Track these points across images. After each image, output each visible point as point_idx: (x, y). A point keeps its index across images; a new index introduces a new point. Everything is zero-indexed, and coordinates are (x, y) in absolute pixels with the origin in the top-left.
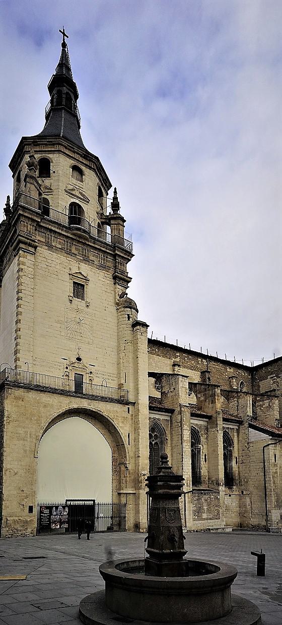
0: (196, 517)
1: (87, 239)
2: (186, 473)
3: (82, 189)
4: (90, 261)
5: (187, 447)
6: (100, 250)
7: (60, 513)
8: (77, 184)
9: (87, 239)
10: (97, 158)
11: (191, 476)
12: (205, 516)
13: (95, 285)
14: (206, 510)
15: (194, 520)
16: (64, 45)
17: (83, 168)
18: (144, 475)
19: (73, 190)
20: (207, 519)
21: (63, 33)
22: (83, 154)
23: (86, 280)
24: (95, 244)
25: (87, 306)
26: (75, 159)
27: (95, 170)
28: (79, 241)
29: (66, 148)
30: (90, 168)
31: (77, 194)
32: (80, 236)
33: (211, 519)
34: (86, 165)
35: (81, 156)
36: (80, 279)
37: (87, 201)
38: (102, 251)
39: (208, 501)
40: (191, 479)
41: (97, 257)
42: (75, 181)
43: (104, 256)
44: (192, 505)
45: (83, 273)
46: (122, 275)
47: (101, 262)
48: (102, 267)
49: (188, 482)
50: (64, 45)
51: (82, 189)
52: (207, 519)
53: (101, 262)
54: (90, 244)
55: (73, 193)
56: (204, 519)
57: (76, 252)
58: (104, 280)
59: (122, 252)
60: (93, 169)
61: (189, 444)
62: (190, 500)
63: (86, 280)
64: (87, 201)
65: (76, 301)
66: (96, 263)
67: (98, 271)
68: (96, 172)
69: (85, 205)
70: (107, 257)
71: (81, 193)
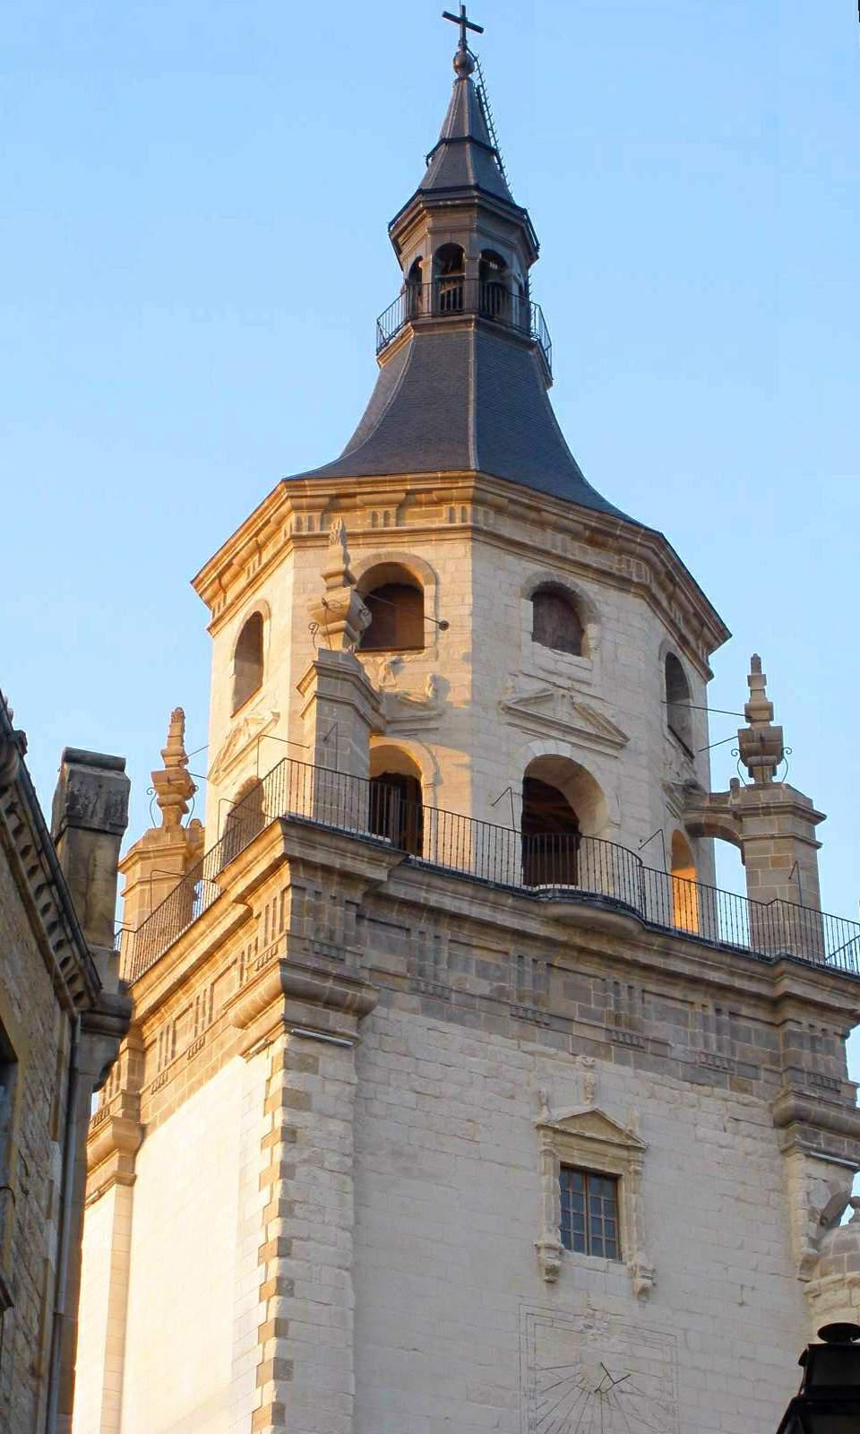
1: (623, 937)
3: (585, 689)
4: (650, 1047)
6: (694, 981)
8: (562, 667)
9: (623, 937)
10: (658, 539)
13: (680, 1168)
16: (465, 65)
17: (587, 588)
21: (463, 21)
22: (586, 527)
23: (628, 1148)
24: (667, 955)
25: (644, 1291)
26: (547, 553)
27: (647, 588)
28: (582, 951)
29: (500, 510)
30: (623, 583)
31: (562, 713)
32: (589, 928)
34: (603, 575)
35: (576, 536)
36: (596, 1146)
37: (616, 741)
38: (709, 984)
41: (682, 1020)
42: (546, 656)
43: (718, 1011)
45: (611, 1116)
46: (828, 1103)
47: (706, 1044)
48: (707, 1071)
50: (465, 65)
51: (585, 689)
53: (706, 1044)
54: (643, 958)
55: (544, 711)
57: (573, 1008)
58: (726, 1138)
59: (814, 983)
60: (639, 585)
63: (628, 1148)
64: (616, 741)
65: (582, 1263)
66: (678, 1050)
67: (691, 1094)
68: (653, 597)
69: (599, 759)
70: (733, 1014)
71: (584, 712)
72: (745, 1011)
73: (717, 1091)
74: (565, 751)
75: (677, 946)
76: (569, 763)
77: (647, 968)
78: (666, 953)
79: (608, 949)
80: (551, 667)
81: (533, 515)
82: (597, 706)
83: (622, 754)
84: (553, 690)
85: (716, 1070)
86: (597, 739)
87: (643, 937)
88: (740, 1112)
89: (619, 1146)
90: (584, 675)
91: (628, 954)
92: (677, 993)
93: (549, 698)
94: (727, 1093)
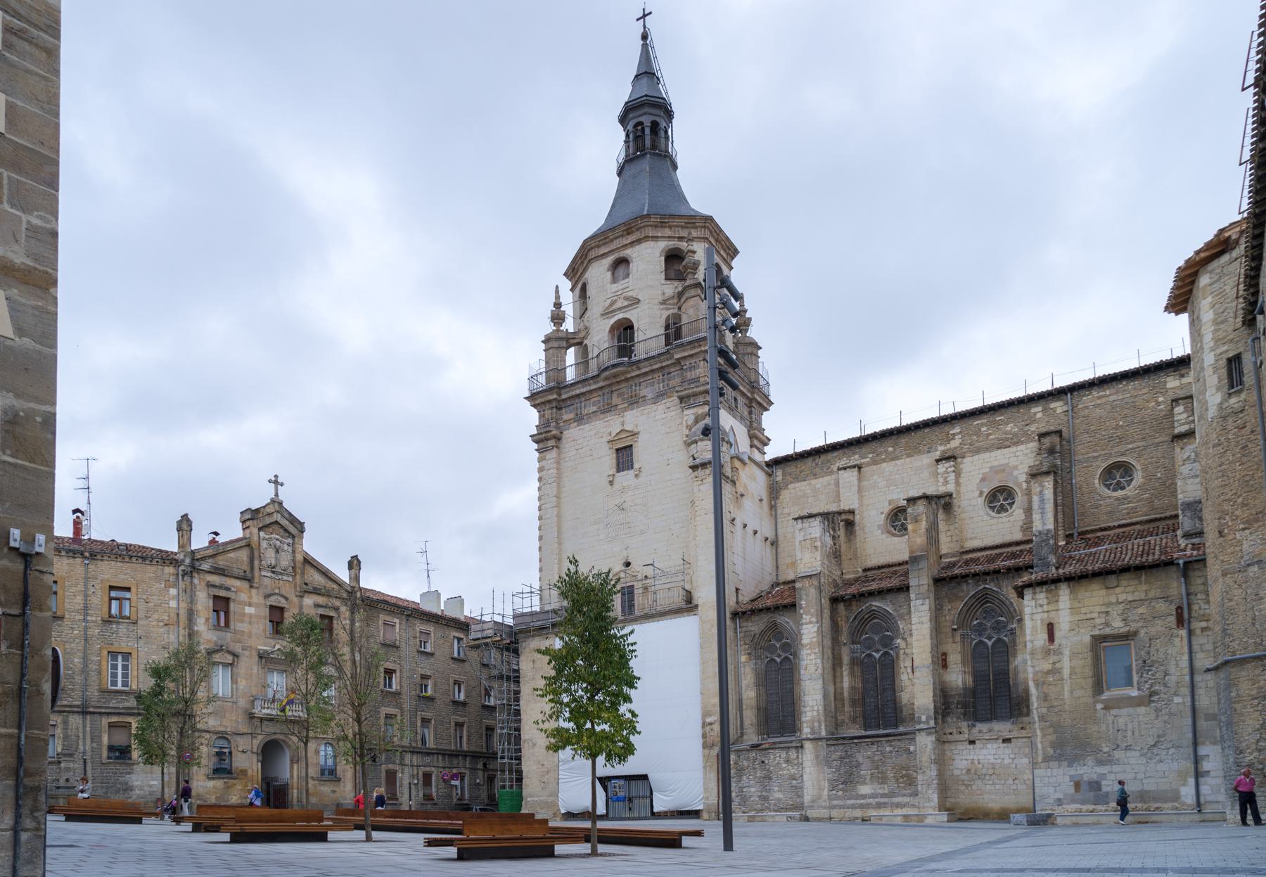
2: (808, 709)
3: (627, 290)
5: (813, 656)
6: (653, 371)
8: (620, 287)
18: (710, 724)
19: (612, 304)
38: (657, 369)
43: (663, 375)
48: (660, 396)
49: (816, 724)
54: (633, 374)
55: (615, 307)
58: (664, 416)
61: (817, 650)
66: (650, 396)
71: (626, 299)
72: (672, 370)
73: (663, 402)
74: (620, 316)
75: (640, 365)
78: (639, 369)
80: (616, 289)
81: (607, 240)
82: (630, 294)
83: (640, 305)
84: (615, 298)
85: (662, 395)
86: (630, 305)
88: (668, 405)
90: (627, 285)
91: (629, 376)
92: (650, 377)
93: (616, 301)
94: (666, 401)
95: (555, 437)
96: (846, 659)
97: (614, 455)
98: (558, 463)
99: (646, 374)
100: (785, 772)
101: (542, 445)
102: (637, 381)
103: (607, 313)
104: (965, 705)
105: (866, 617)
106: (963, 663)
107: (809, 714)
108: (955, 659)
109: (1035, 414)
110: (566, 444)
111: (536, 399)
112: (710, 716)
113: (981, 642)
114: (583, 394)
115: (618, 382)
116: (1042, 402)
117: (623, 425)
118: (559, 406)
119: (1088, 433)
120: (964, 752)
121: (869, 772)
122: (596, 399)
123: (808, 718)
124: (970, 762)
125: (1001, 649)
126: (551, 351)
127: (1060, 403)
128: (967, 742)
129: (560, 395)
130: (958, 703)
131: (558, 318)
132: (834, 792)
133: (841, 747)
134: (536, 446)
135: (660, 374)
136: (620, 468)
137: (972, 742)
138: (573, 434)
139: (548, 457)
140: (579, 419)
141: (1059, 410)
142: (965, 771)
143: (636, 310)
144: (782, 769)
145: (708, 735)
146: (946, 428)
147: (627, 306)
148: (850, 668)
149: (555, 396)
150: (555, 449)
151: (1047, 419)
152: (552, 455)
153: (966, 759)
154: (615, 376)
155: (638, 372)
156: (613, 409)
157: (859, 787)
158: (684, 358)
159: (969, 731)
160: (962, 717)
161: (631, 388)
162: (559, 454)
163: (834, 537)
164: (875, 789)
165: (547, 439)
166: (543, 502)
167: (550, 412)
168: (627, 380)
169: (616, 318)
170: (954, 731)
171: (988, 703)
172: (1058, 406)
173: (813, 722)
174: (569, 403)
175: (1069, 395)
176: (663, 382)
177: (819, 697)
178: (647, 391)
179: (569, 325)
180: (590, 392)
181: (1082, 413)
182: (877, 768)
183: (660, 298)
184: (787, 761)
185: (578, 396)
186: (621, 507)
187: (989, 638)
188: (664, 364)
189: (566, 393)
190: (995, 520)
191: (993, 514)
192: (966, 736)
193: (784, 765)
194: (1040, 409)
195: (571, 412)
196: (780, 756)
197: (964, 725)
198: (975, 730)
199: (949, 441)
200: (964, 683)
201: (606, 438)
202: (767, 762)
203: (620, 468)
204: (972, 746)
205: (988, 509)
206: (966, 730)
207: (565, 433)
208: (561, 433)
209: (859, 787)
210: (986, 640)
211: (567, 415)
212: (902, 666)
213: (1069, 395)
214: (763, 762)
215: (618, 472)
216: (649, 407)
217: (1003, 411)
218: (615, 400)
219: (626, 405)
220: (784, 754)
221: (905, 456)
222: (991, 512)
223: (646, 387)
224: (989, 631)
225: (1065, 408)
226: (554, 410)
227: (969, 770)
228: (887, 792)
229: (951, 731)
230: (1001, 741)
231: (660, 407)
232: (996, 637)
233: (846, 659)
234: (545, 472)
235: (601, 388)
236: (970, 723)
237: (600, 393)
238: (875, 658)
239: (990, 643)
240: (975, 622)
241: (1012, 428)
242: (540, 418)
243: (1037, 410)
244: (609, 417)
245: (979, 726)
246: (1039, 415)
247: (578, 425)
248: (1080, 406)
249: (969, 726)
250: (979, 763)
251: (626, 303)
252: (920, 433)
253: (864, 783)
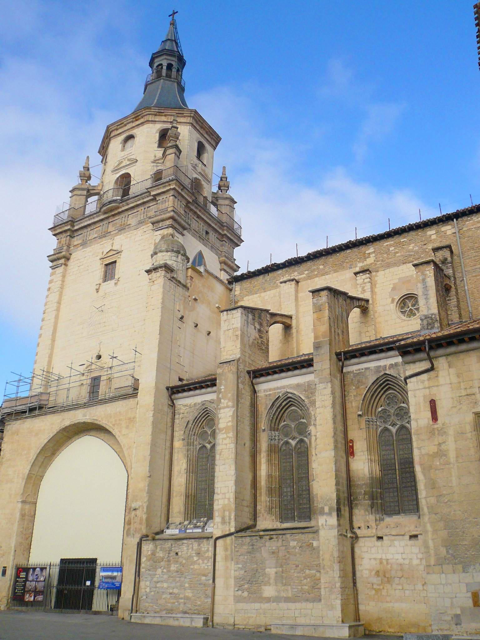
0: (246, 594)
1: (118, 208)
2: (220, 496)
7: (37, 578)
11: (232, 500)
12: (269, 591)
14: (273, 576)
15: (238, 600)
20: (277, 600)
33: (287, 600)
39: (281, 554)
40: (233, 506)
44: (233, 566)
49: (227, 513)
52: (277, 600)
54: (123, 209)
56: (268, 600)
62: (229, 553)
75: (128, 202)
76: (125, 173)
77: (127, 210)
78: (128, 204)
79: (116, 212)
87: (121, 204)
89: (116, 254)
91: (120, 210)
95: (64, 257)
96: (264, 445)
97: (103, 269)
98: (64, 276)
99: (133, 208)
100: (196, 567)
101: (55, 263)
102: (126, 214)
103: (115, 170)
104: (372, 498)
105: (283, 404)
106: (369, 449)
107: (221, 502)
108: (360, 446)
109: (430, 236)
110: (70, 263)
111: (56, 230)
112: (136, 501)
113: (386, 429)
114: (89, 225)
115: (113, 215)
116: (435, 227)
117: (112, 246)
118: (72, 233)
119: (473, 249)
120: (373, 550)
121: (275, 570)
122: (98, 229)
123: (220, 507)
124: (378, 561)
125: (405, 437)
126: (74, 197)
127: (449, 227)
128: (375, 538)
129: (73, 226)
130: (365, 494)
131: (86, 176)
132: (240, 592)
133: (248, 539)
134: (51, 264)
135: (143, 208)
136: (105, 279)
137: (380, 538)
138: (78, 255)
139: (57, 272)
140: (84, 244)
141: (449, 232)
142: (374, 573)
143: (134, 167)
144: (194, 563)
145: (132, 521)
146: (363, 248)
147: (129, 165)
148: (268, 455)
149: (69, 227)
150: (63, 266)
151: (440, 240)
152: (60, 270)
153: (375, 559)
154: (111, 210)
155: (126, 207)
156: (107, 235)
157: (263, 587)
158: (159, 194)
159: (377, 526)
160: (369, 509)
161: (122, 219)
162: (65, 270)
163: (260, 331)
164: (279, 592)
165: (59, 259)
166: (47, 307)
167: (65, 239)
168: (119, 213)
169: (121, 173)
170: (362, 525)
171: (396, 494)
172: (448, 229)
173: (224, 511)
174: (80, 232)
175: (455, 220)
176: (144, 213)
177: (231, 484)
178: (132, 220)
179: (93, 182)
180: (94, 223)
181: (467, 235)
182: (281, 566)
183: (153, 158)
184: (198, 554)
185: (85, 227)
186: (100, 309)
187: (394, 425)
188: (145, 200)
189: (77, 225)
190: (406, 322)
191: (405, 318)
192: (374, 531)
193: (195, 559)
194: (434, 232)
195: (80, 240)
196: (192, 548)
197: (371, 518)
198: (383, 524)
199: (365, 259)
200: (371, 472)
201: (99, 258)
202: (180, 554)
203: (105, 279)
204: (379, 543)
205: (400, 314)
206: (372, 524)
207: (73, 254)
208: (71, 254)
209: (263, 587)
210: (390, 427)
211: (76, 241)
212: (314, 453)
213: (455, 220)
214: (177, 554)
215: (105, 281)
216: (132, 232)
217: (406, 234)
218: (111, 228)
219: (117, 231)
220: (195, 545)
221: (333, 272)
222: (402, 316)
223: (132, 218)
224: (392, 418)
225: (453, 230)
226: (68, 237)
227: (378, 571)
228: (290, 595)
229: (359, 525)
230: (408, 537)
231: (140, 232)
232: (399, 423)
233: (264, 445)
234: (53, 284)
235: (102, 220)
236: (378, 516)
237: (101, 224)
238: (291, 445)
239: (394, 430)
240: (380, 409)
241: (414, 247)
242: (58, 243)
243: (431, 232)
244: (104, 241)
245: (388, 520)
246: (434, 237)
247: (83, 248)
248: (465, 229)
249: (376, 520)
250: (387, 564)
251: (128, 163)
252: (343, 253)
253: (268, 583)
